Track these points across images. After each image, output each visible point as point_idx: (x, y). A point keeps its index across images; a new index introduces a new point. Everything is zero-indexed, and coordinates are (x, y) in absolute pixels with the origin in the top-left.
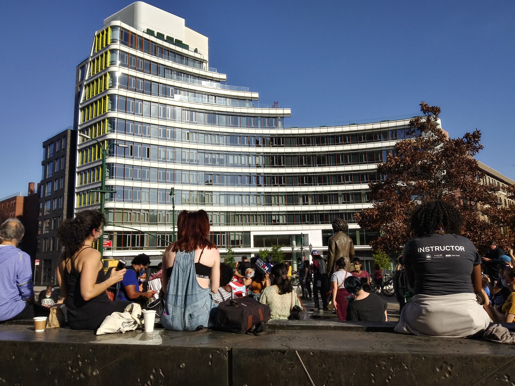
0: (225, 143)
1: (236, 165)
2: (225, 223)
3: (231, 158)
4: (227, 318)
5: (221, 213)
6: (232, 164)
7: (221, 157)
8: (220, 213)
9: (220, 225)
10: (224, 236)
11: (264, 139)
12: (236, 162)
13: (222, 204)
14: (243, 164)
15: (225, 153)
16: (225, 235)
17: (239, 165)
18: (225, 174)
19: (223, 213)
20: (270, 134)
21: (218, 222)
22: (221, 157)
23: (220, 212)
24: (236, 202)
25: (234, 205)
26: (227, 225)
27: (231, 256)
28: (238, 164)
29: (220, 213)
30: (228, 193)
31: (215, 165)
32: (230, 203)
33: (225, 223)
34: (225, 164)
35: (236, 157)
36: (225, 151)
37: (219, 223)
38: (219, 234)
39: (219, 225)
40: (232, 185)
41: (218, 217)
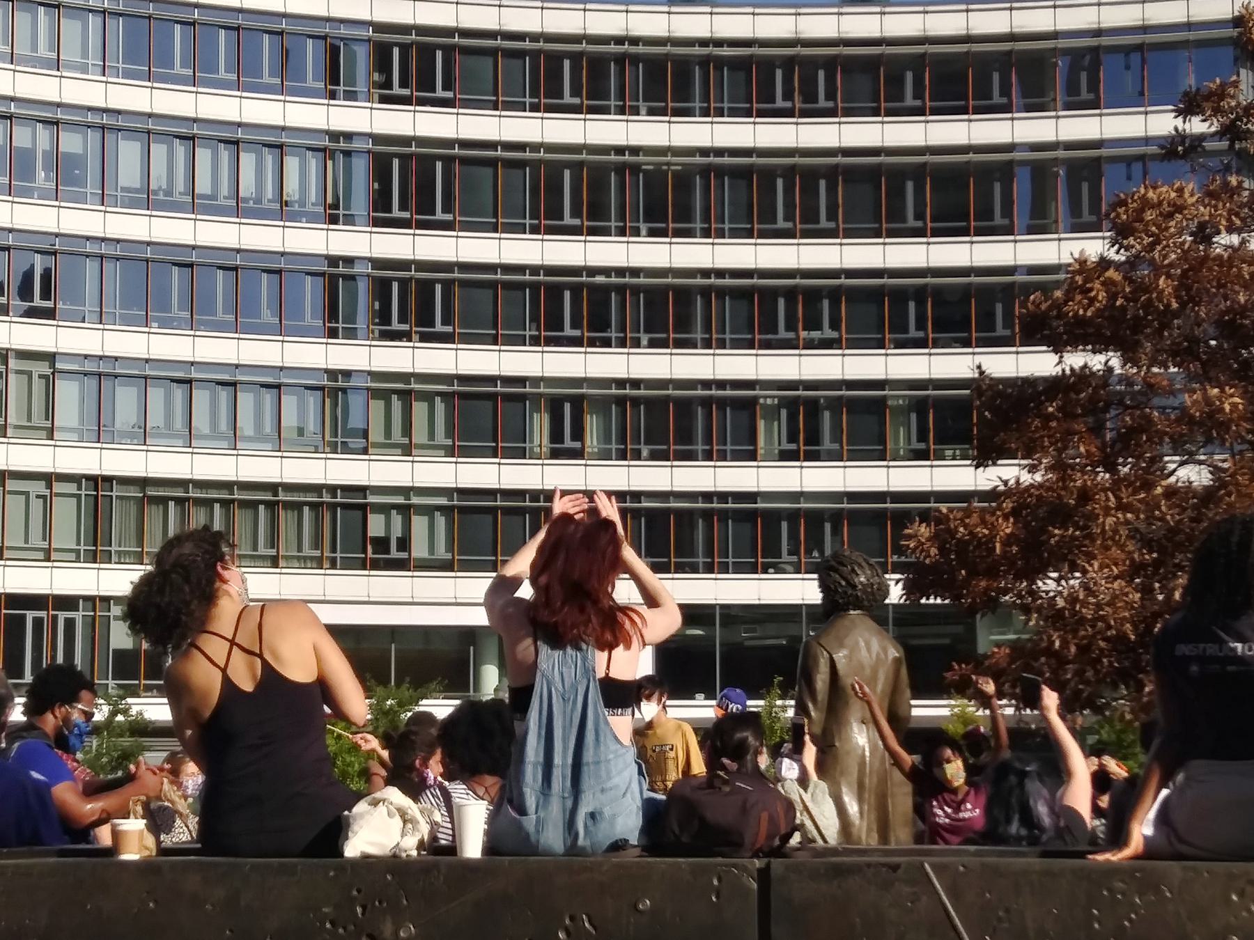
0: (94, 60)
1: (161, 197)
2: (82, 548)
3: (128, 153)
4: (702, 820)
5: (58, 487)
6: (136, 191)
7: (71, 142)
8: (50, 486)
9: (48, 559)
10: (70, 624)
11: (334, 52)
12: (159, 178)
13: (63, 429)
14: (203, 197)
15: (90, 118)
16: (78, 616)
17: (177, 197)
18: (90, 248)
19: (71, 488)
20: (370, 23)
21: (36, 541)
22: (71, 142)
23: (48, 478)
24: (156, 418)
25: (142, 435)
26: (93, 557)
27: (126, 742)
28: (169, 193)
29: (50, 486)
30: (104, 368)
31: (26, 193)
32: (118, 425)
33: (82, 548)
34: (92, 188)
35: (159, 151)
36: (90, 109)
37: (45, 545)
38: (43, 614)
39: (41, 555)
40: (128, 321)
41: (36, 506)
